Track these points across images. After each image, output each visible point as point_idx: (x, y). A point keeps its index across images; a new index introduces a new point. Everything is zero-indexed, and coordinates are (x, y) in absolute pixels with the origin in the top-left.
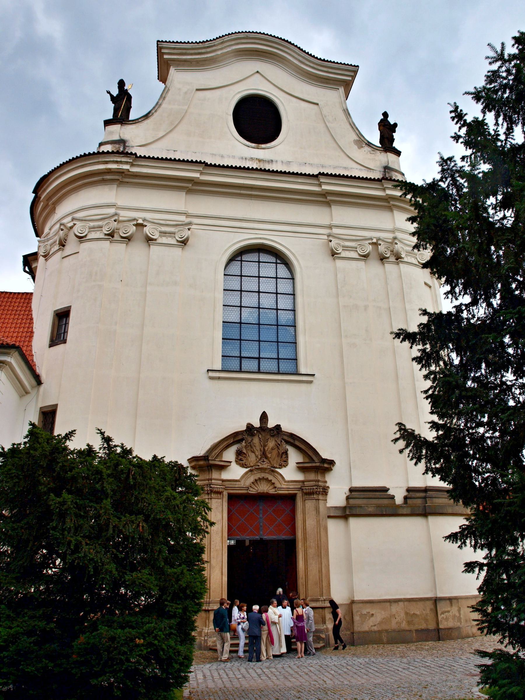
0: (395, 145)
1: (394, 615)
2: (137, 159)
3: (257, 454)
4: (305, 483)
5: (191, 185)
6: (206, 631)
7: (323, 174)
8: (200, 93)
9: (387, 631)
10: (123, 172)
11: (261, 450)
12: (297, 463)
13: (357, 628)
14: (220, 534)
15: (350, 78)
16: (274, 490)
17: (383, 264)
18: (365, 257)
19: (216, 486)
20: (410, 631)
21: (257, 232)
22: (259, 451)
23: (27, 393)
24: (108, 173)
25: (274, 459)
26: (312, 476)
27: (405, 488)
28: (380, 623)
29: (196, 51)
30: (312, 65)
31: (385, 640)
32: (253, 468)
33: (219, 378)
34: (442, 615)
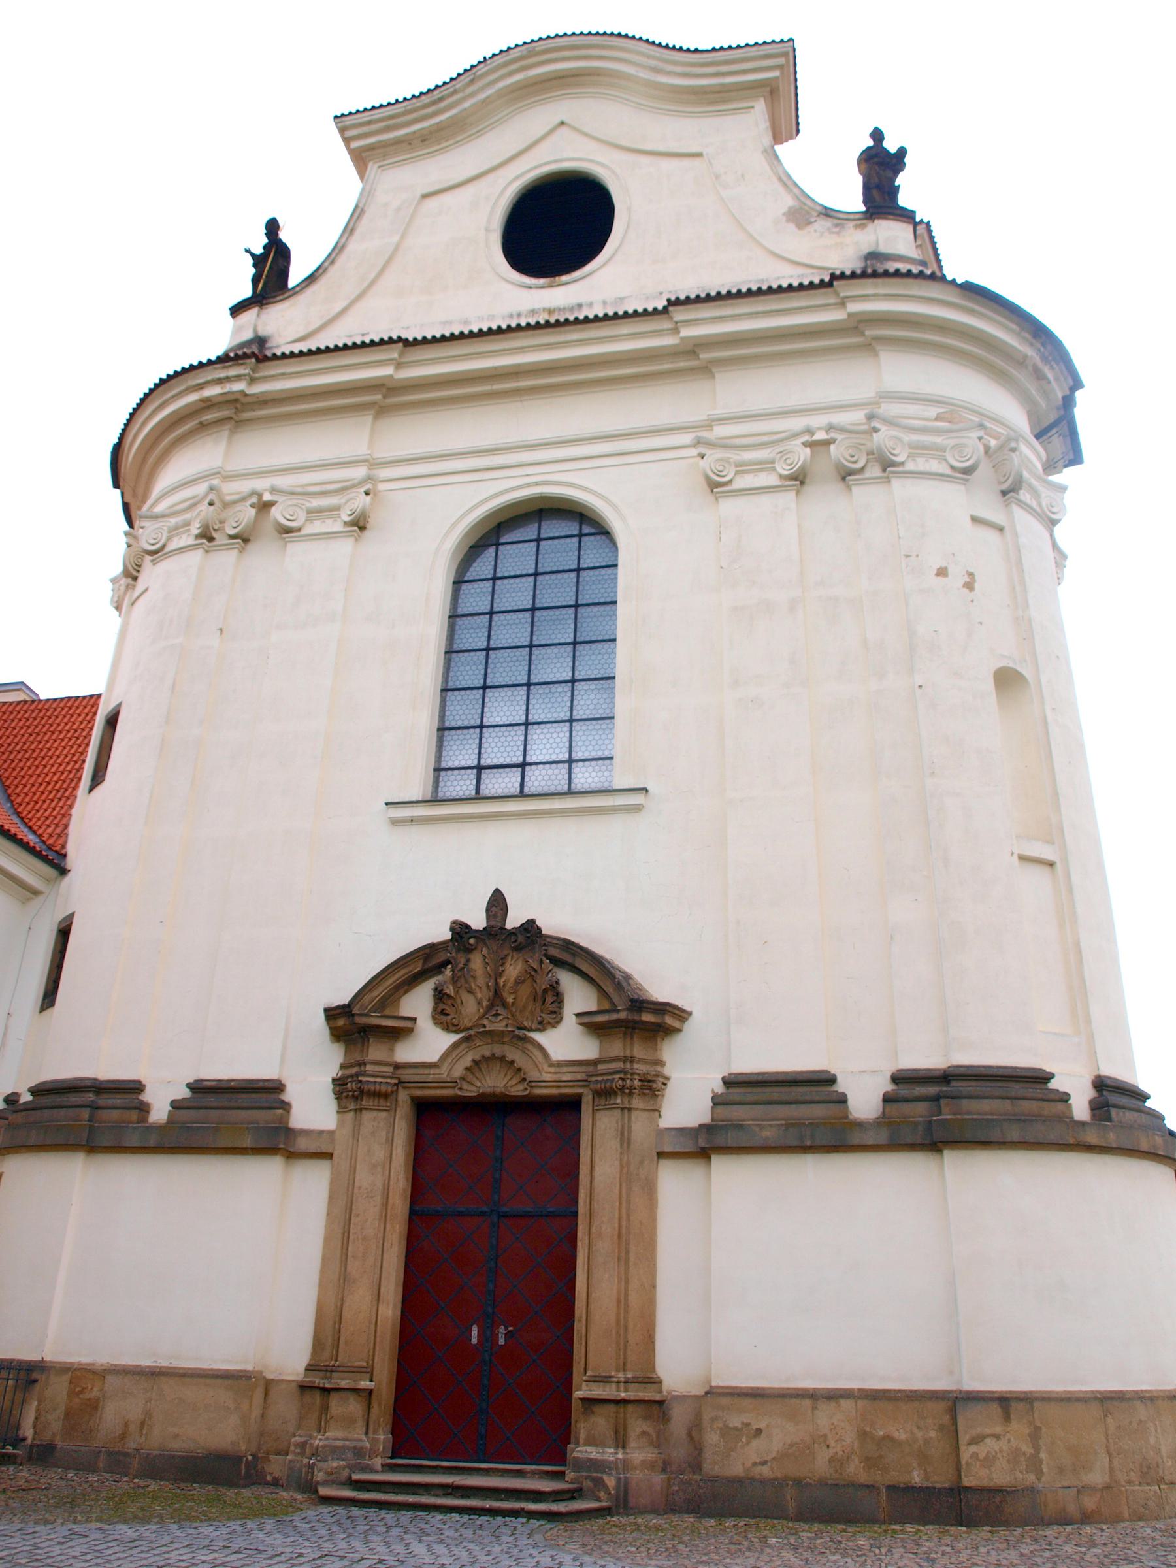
0: (904, 200)
1: (825, 1436)
2: (261, 365)
3: (479, 995)
4: (600, 1067)
5: (380, 396)
6: (317, 1442)
7: (677, 302)
8: (432, 203)
9: (799, 1483)
10: (236, 400)
11: (488, 987)
12: (578, 1015)
13: (712, 1466)
14: (378, 1199)
15: (776, 73)
16: (521, 1087)
17: (849, 488)
18: (799, 479)
19: (372, 1079)
20: (870, 1487)
21: (529, 470)
22: (484, 989)
23: (36, 893)
24: (208, 407)
25: (524, 1007)
26: (617, 1048)
27: (888, 1075)
28: (782, 1456)
29: (414, 115)
30: (679, 69)
31: (791, 1511)
32: (472, 1032)
33: (412, 820)
34: (973, 1448)
